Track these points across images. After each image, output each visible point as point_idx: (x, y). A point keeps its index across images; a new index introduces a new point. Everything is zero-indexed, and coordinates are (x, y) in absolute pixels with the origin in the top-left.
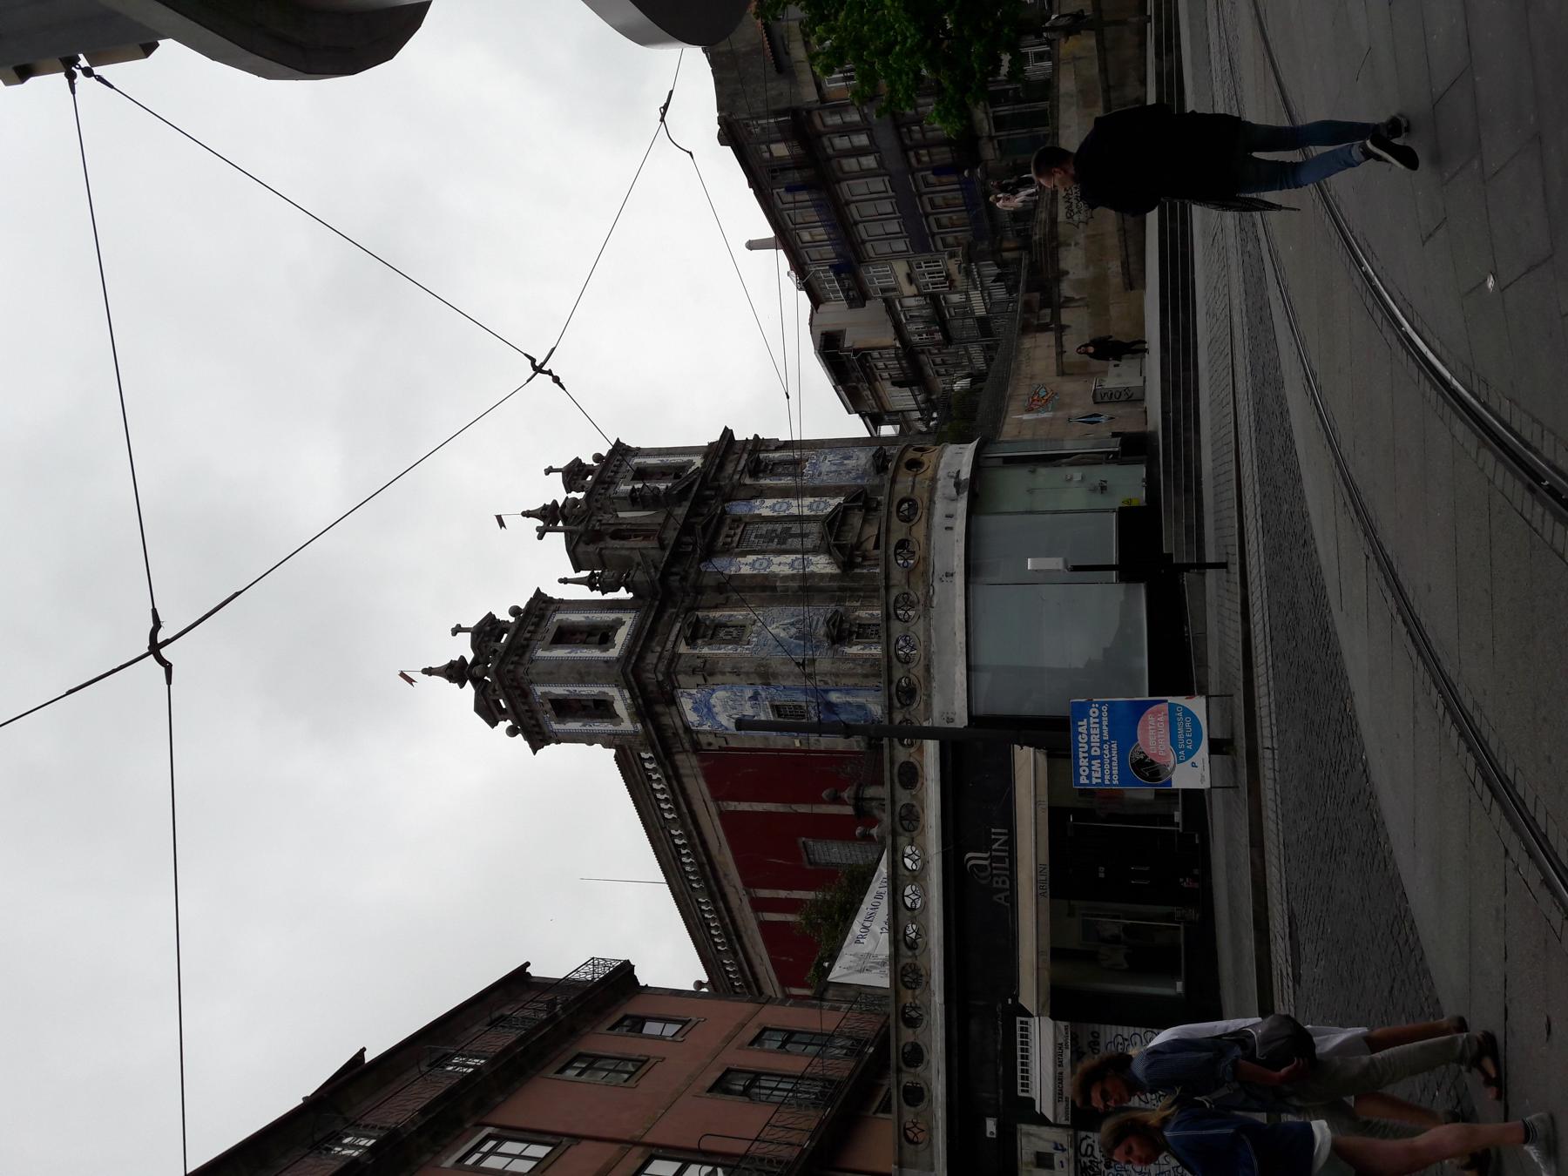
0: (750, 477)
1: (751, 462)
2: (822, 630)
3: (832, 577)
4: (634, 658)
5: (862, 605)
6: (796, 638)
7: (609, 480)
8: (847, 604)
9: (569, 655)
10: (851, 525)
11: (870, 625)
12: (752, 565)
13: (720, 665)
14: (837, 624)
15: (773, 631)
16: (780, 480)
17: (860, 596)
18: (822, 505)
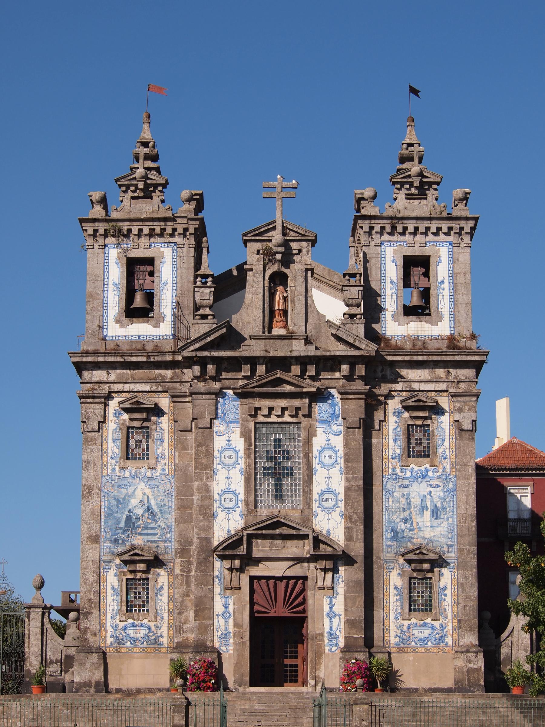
0: (402, 402)
1: (419, 400)
2: (138, 541)
3: (208, 540)
4: (89, 359)
5: (176, 577)
6: (129, 518)
7: (400, 229)
8: (178, 560)
9: (111, 283)
10: (284, 547)
11: (148, 589)
12: (229, 447)
13: (91, 447)
14: (136, 558)
15: (139, 490)
16: (395, 441)
17: (190, 571)
18: (330, 504)
